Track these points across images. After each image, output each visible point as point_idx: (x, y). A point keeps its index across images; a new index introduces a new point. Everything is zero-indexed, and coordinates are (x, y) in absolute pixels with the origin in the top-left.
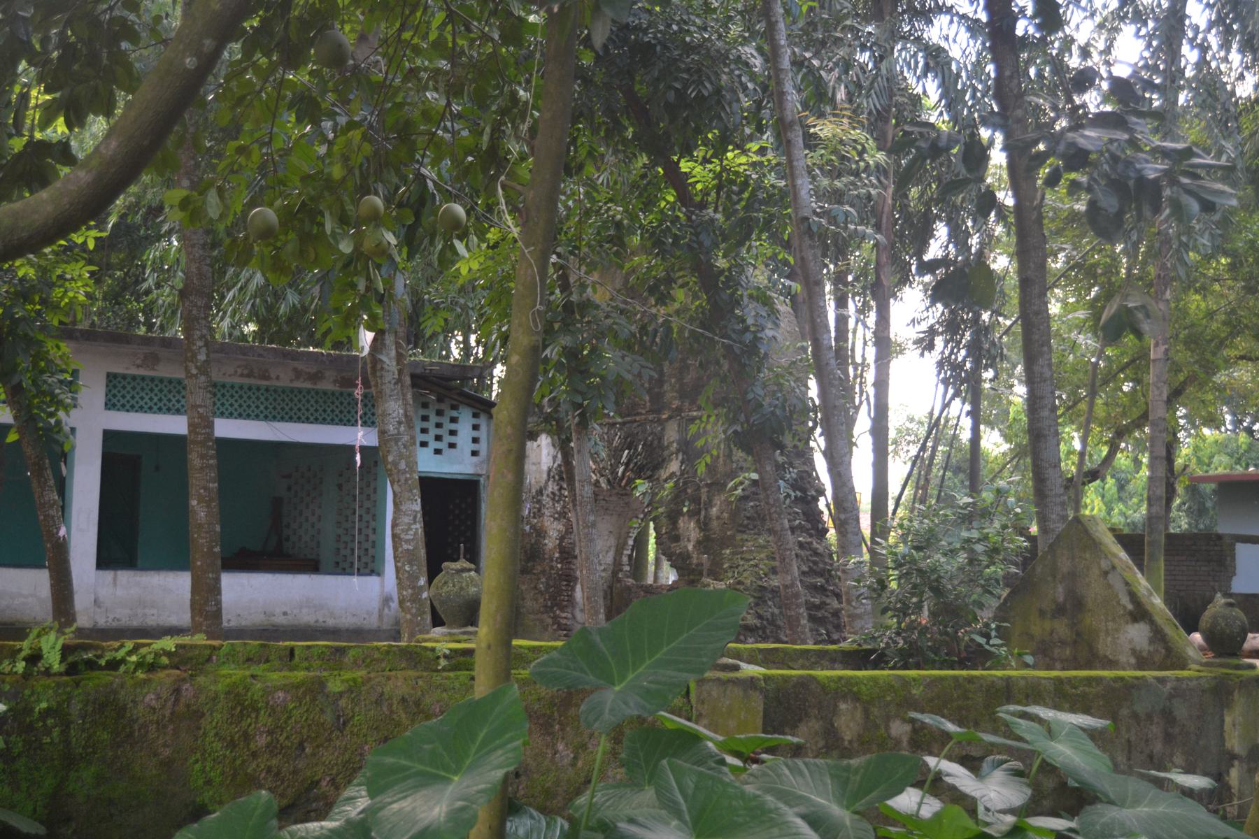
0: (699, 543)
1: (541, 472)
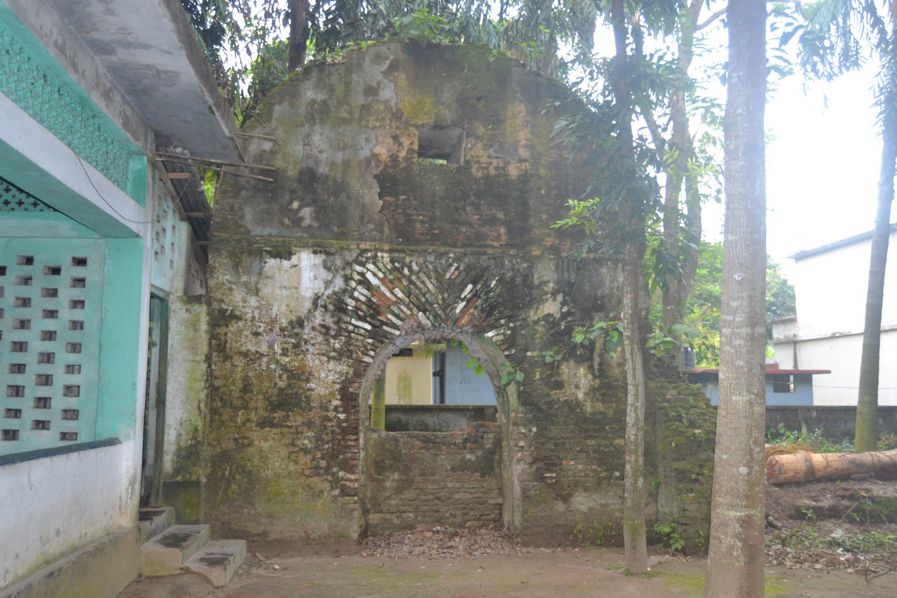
0: (593, 390)
1: (299, 299)
